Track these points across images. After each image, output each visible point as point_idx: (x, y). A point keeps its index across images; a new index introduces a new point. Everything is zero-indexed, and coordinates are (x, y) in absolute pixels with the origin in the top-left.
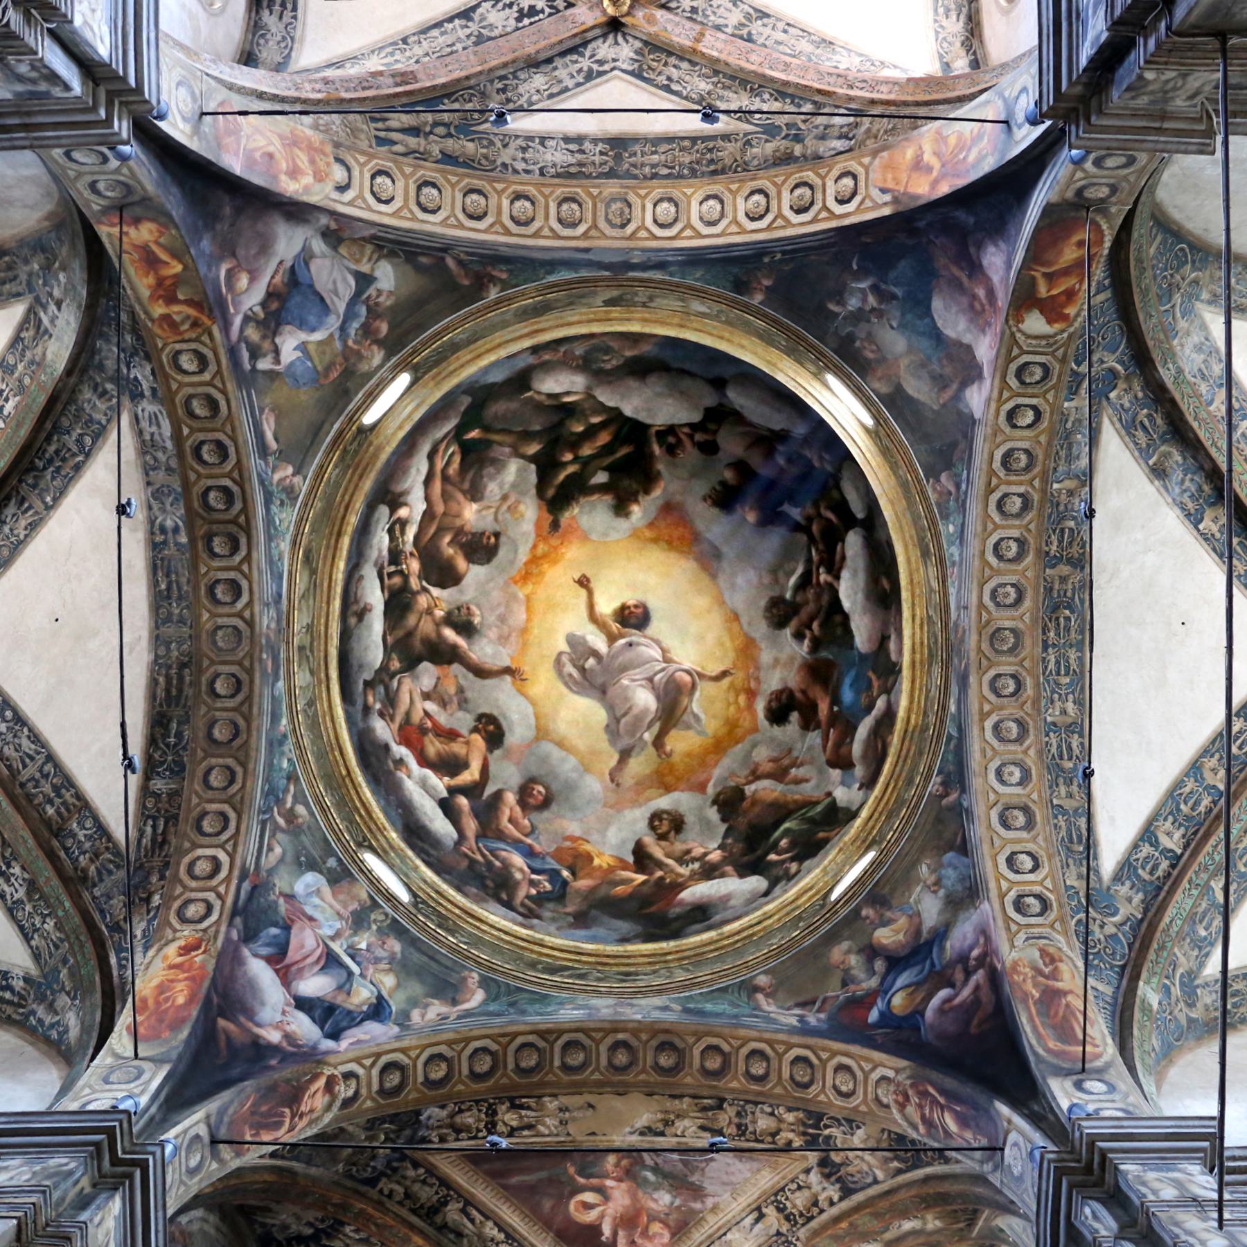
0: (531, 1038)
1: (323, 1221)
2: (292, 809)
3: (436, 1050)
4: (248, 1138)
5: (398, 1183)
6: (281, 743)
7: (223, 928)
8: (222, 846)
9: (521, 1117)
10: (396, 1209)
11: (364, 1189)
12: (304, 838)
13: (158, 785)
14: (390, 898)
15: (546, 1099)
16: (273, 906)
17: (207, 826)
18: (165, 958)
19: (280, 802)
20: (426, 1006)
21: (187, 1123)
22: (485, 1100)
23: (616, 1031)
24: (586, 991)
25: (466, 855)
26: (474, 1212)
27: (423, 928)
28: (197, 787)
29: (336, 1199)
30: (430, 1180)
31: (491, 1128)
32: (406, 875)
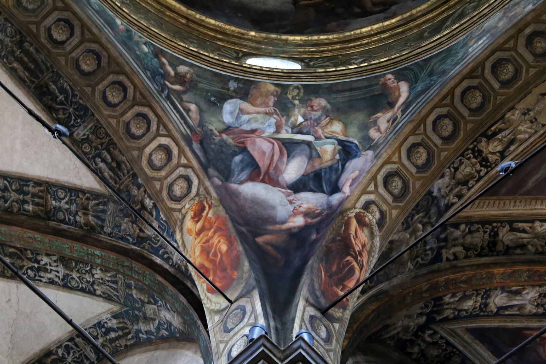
0: (465, 84)
1: (426, 306)
2: (176, 73)
3: (408, 144)
4: (342, 294)
5: (454, 246)
6: (130, 37)
7: (208, 183)
8: (158, 135)
9: (500, 141)
10: (467, 262)
11: (435, 267)
12: (201, 85)
13: (81, 132)
14: (289, 74)
15: (508, 115)
16: (223, 144)
17: (135, 130)
18: (190, 231)
19: (165, 76)
20: (375, 122)
21: (299, 314)
22: (467, 149)
23: (521, 30)
24: (475, 23)
25: (308, 6)
26: (520, 225)
27: (328, 76)
29: (425, 286)
30: (473, 229)
31: (485, 163)
32: (284, 52)
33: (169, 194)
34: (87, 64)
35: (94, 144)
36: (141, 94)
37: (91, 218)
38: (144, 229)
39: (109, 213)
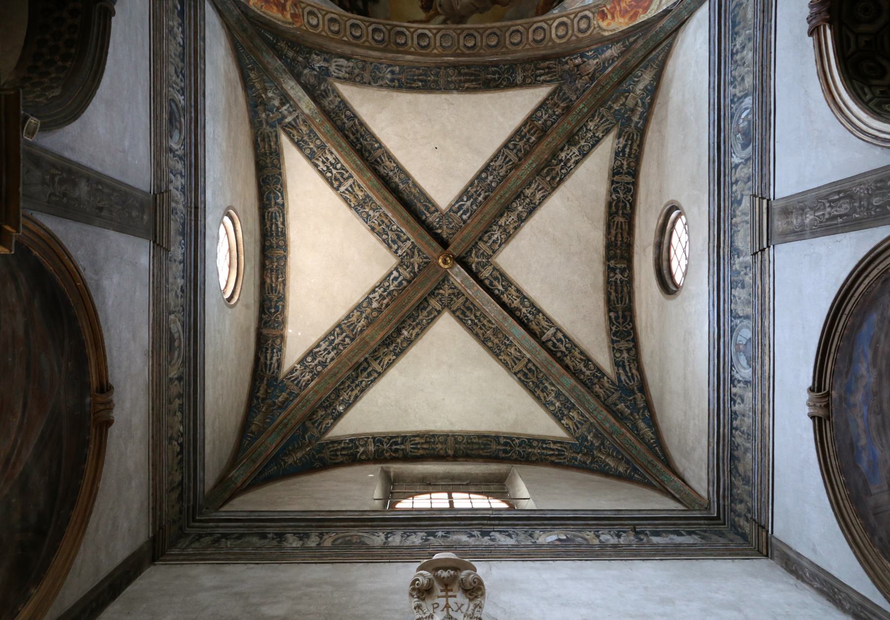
8: (550, 26)
28: (521, 48)
33: (582, 33)
34: (493, 41)
35: (530, 75)
36: (526, 23)
37: (562, 105)
38: (588, 72)
39: (567, 91)
